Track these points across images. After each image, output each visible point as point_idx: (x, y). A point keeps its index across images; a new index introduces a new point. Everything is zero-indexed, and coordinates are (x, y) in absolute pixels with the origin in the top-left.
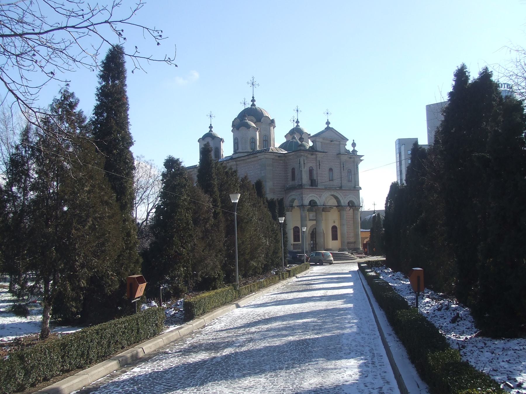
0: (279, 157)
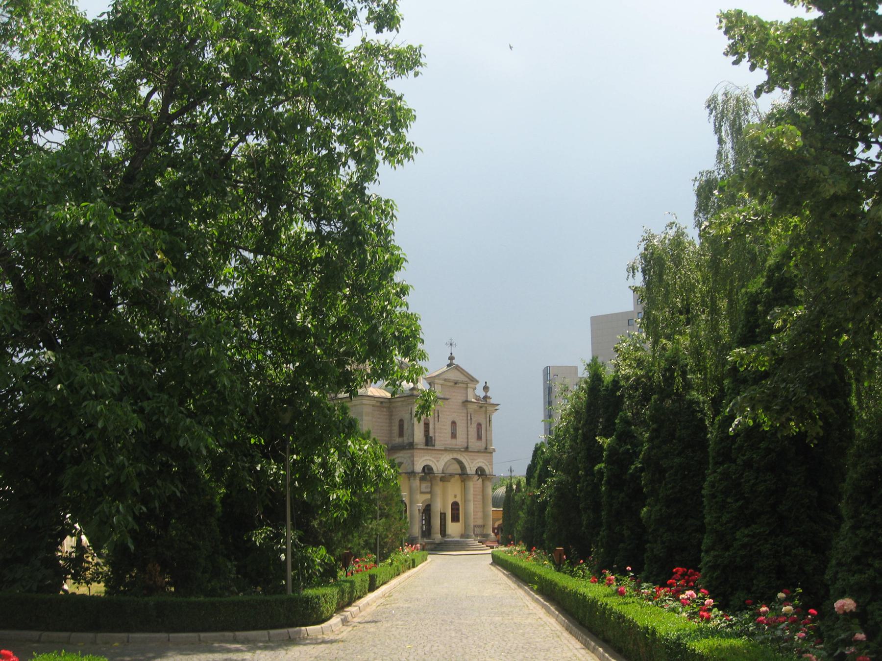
0: (382, 402)
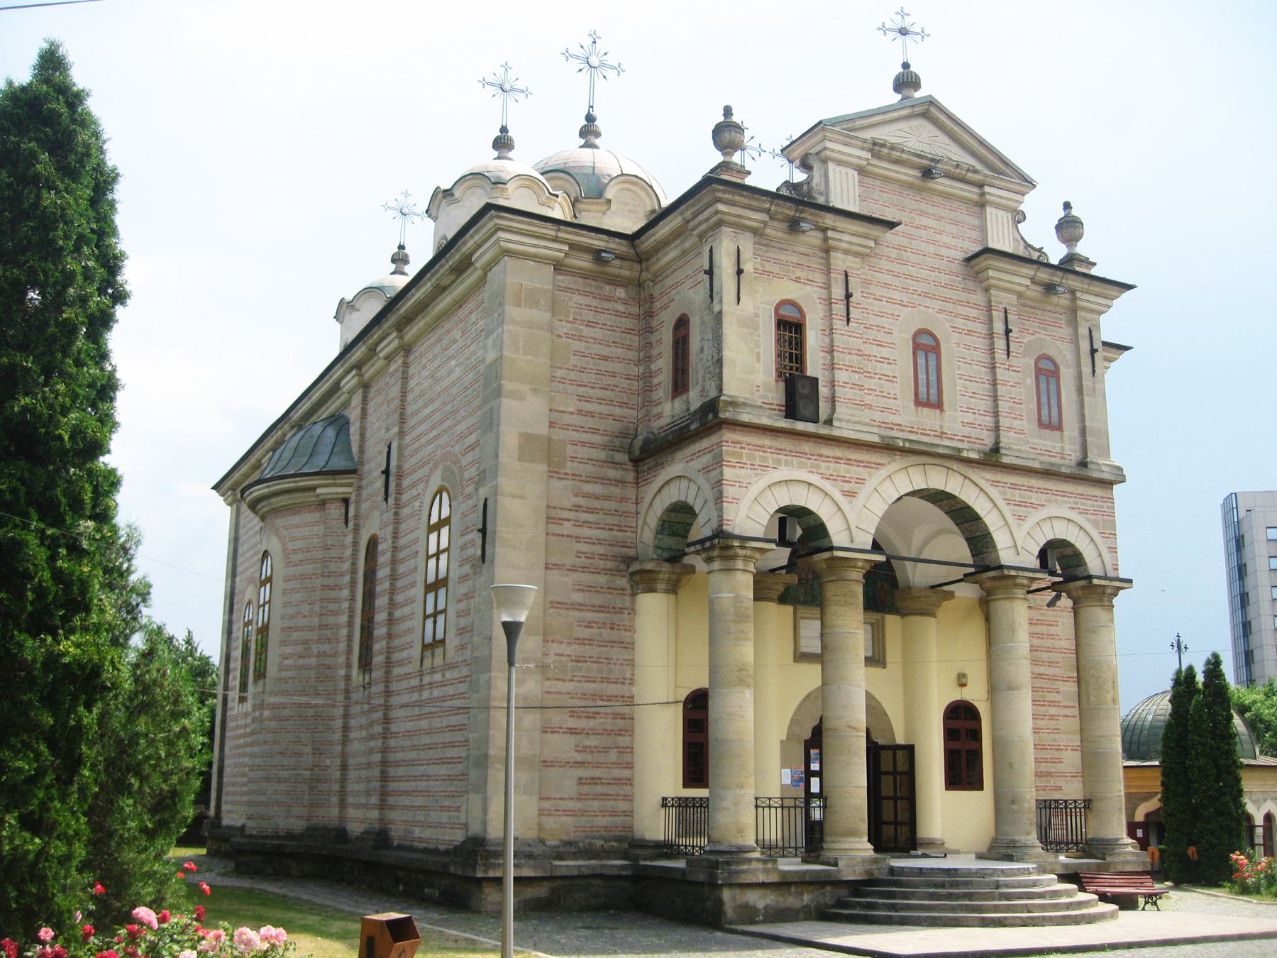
0: (597, 254)
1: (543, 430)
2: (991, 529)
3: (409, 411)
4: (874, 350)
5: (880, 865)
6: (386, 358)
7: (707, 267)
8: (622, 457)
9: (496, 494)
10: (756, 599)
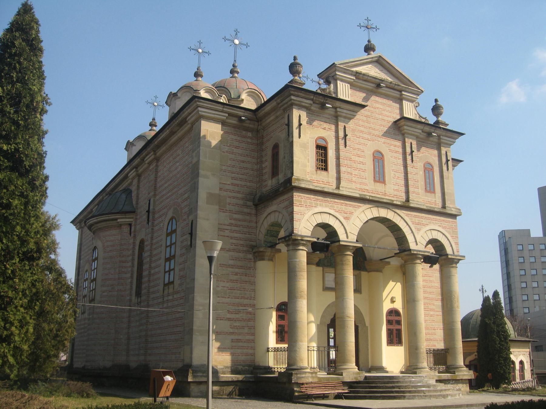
1: (217, 191)
2: (406, 234)
3: (158, 185)
4: (357, 159)
5: (361, 375)
6: (148, 163)
7: (287, 122)
8: (250, 203)
9: (197, 218)
10: (307, 264)
